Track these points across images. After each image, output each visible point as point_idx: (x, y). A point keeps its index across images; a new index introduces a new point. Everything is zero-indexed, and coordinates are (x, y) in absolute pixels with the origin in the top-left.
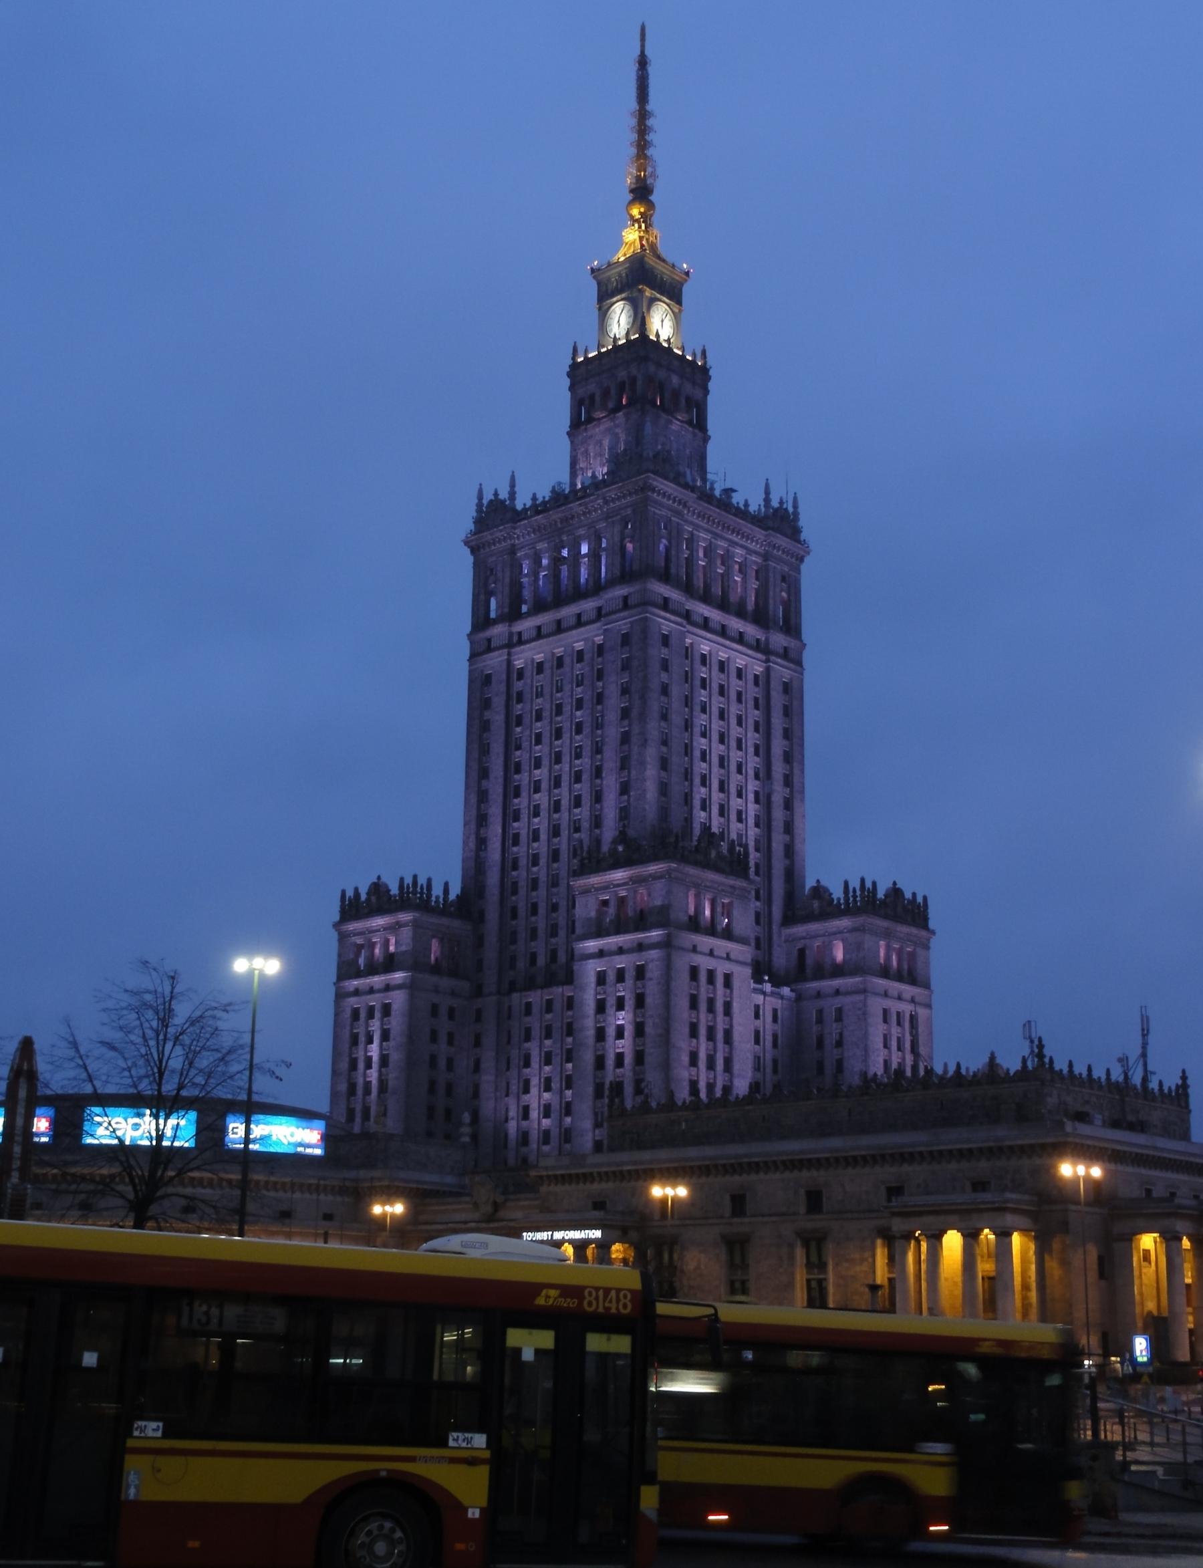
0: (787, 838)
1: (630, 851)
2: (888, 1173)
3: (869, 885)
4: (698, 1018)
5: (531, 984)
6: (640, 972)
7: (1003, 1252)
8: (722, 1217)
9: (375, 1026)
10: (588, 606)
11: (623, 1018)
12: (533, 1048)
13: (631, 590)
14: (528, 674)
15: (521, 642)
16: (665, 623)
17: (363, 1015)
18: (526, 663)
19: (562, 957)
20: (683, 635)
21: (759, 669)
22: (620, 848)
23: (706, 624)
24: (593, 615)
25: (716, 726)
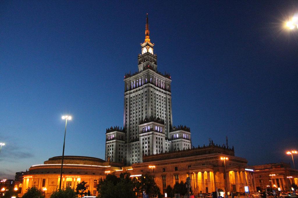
1: (147, 120)
2: (188, 163)
3: (181, 126)
5: (133, 141)
6: (149, 138)
7: (209, 175)
9: (111, 148)
10: (140, 88)
11: (147, 145)
14: (132, 97)
15: (131, 93)
16: (152, 89)
17: (109, 146)
19: (138, 137)
21: (165, 96)
23: (157, 90)
24: (141, 89)
25: (159, 104)
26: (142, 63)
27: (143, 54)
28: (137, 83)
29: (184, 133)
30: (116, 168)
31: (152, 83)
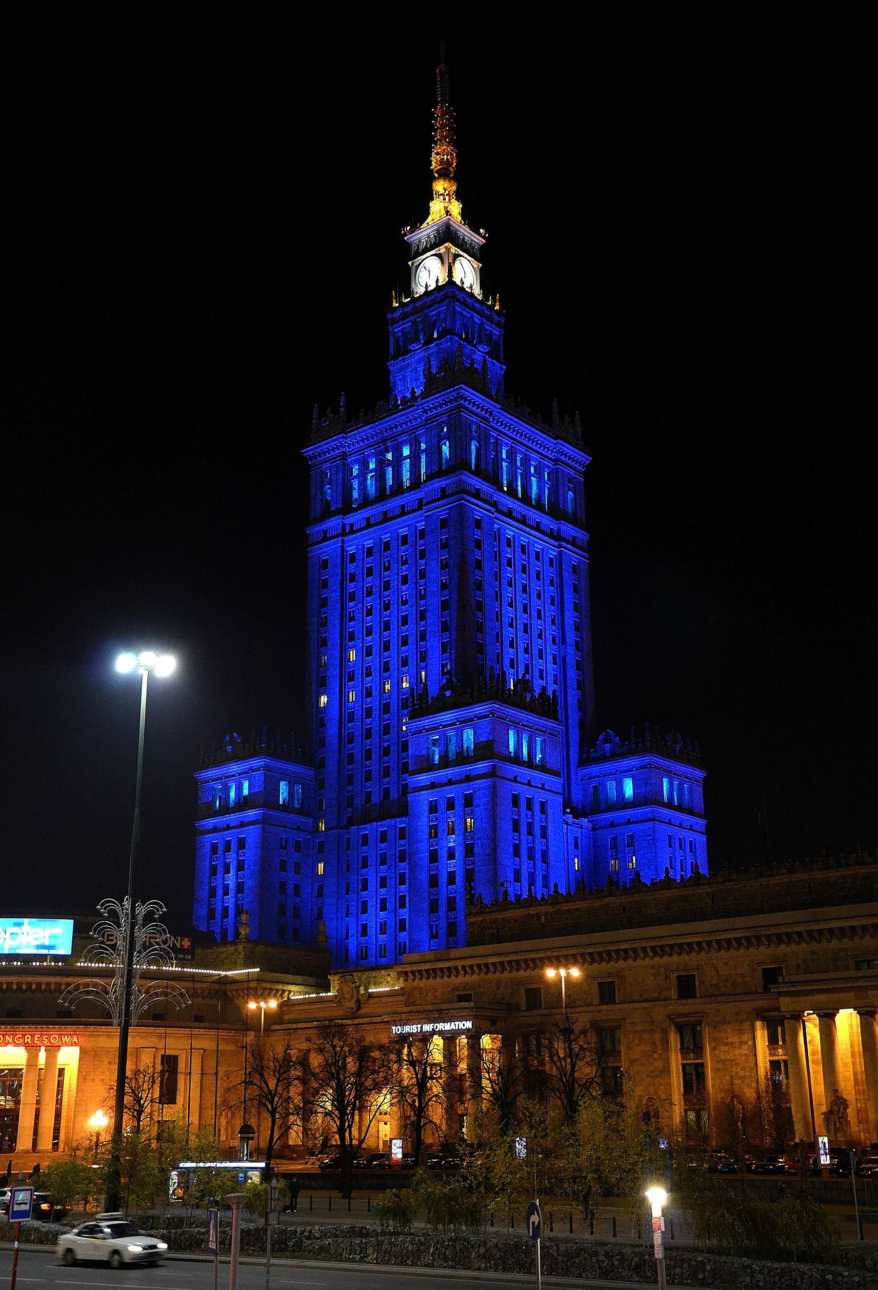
4: (520, 842)
5: (366, 820)
8: (590, 1005)
9: (231, 858)
10: (410, 498)
12: (372, 874)
14: (359, 557)
15: (352, 532)
16: (479, 510)
17: (221, 849)
19: (394, 795)
20: (491, 521)
22: (448, 693)
23: (509, 514)
25: (521, 599)
26: (414, 346)
27: (420, 290)
28: (389, 472)
29: (668, 773)
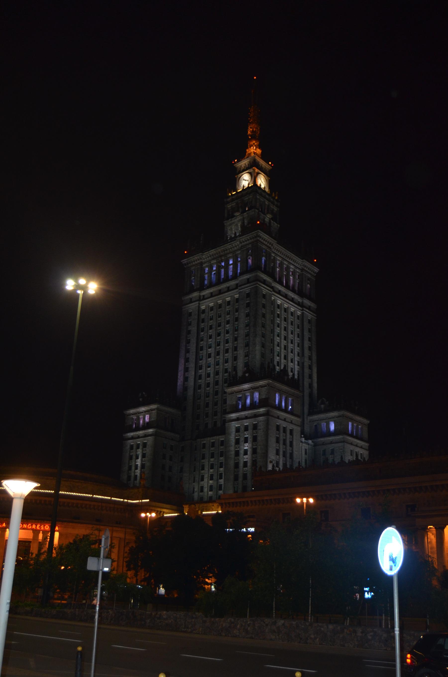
0: (310, 380)
1: (251, 375)
4: (279, 447)
9: (140, 452)
10: (233, 283)
12: (206, 462)
13: (251, 276)
15: (204, 299)
16: (265, 290)
18: (206, 307)
19: (219, 424)
20: (271, 295)
23: (279, 292)
25: (283, 333)
26: (237, 214)
29: (352, 420)
30: (165, 505)
31: (265, 272)
